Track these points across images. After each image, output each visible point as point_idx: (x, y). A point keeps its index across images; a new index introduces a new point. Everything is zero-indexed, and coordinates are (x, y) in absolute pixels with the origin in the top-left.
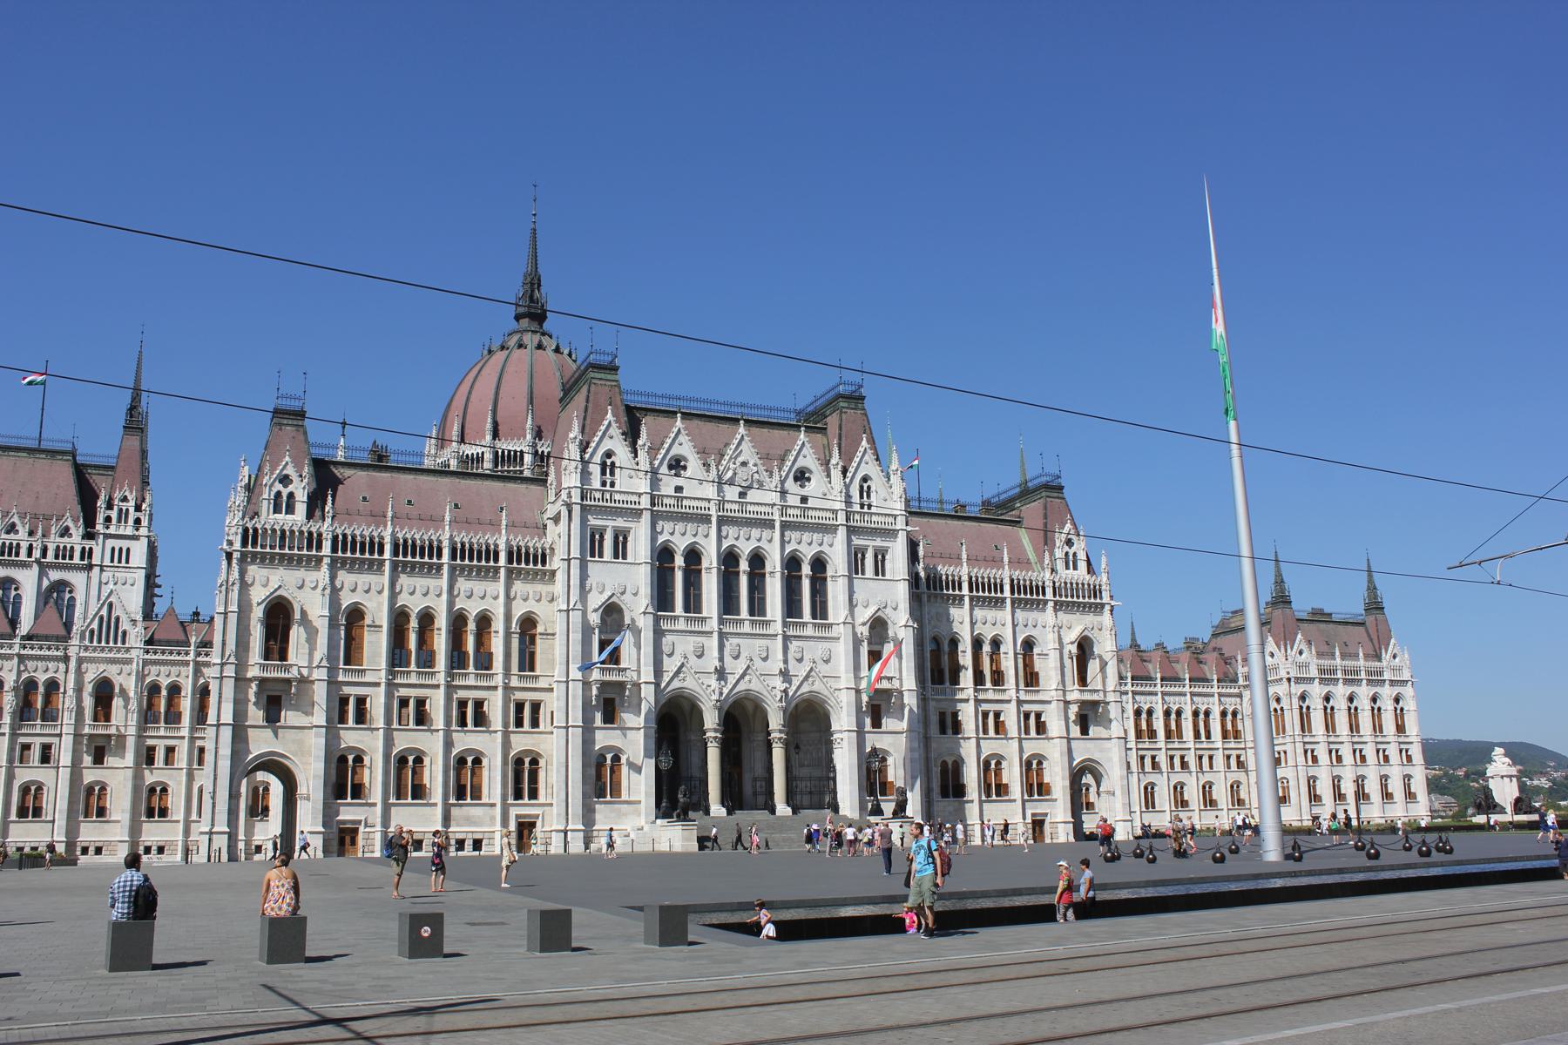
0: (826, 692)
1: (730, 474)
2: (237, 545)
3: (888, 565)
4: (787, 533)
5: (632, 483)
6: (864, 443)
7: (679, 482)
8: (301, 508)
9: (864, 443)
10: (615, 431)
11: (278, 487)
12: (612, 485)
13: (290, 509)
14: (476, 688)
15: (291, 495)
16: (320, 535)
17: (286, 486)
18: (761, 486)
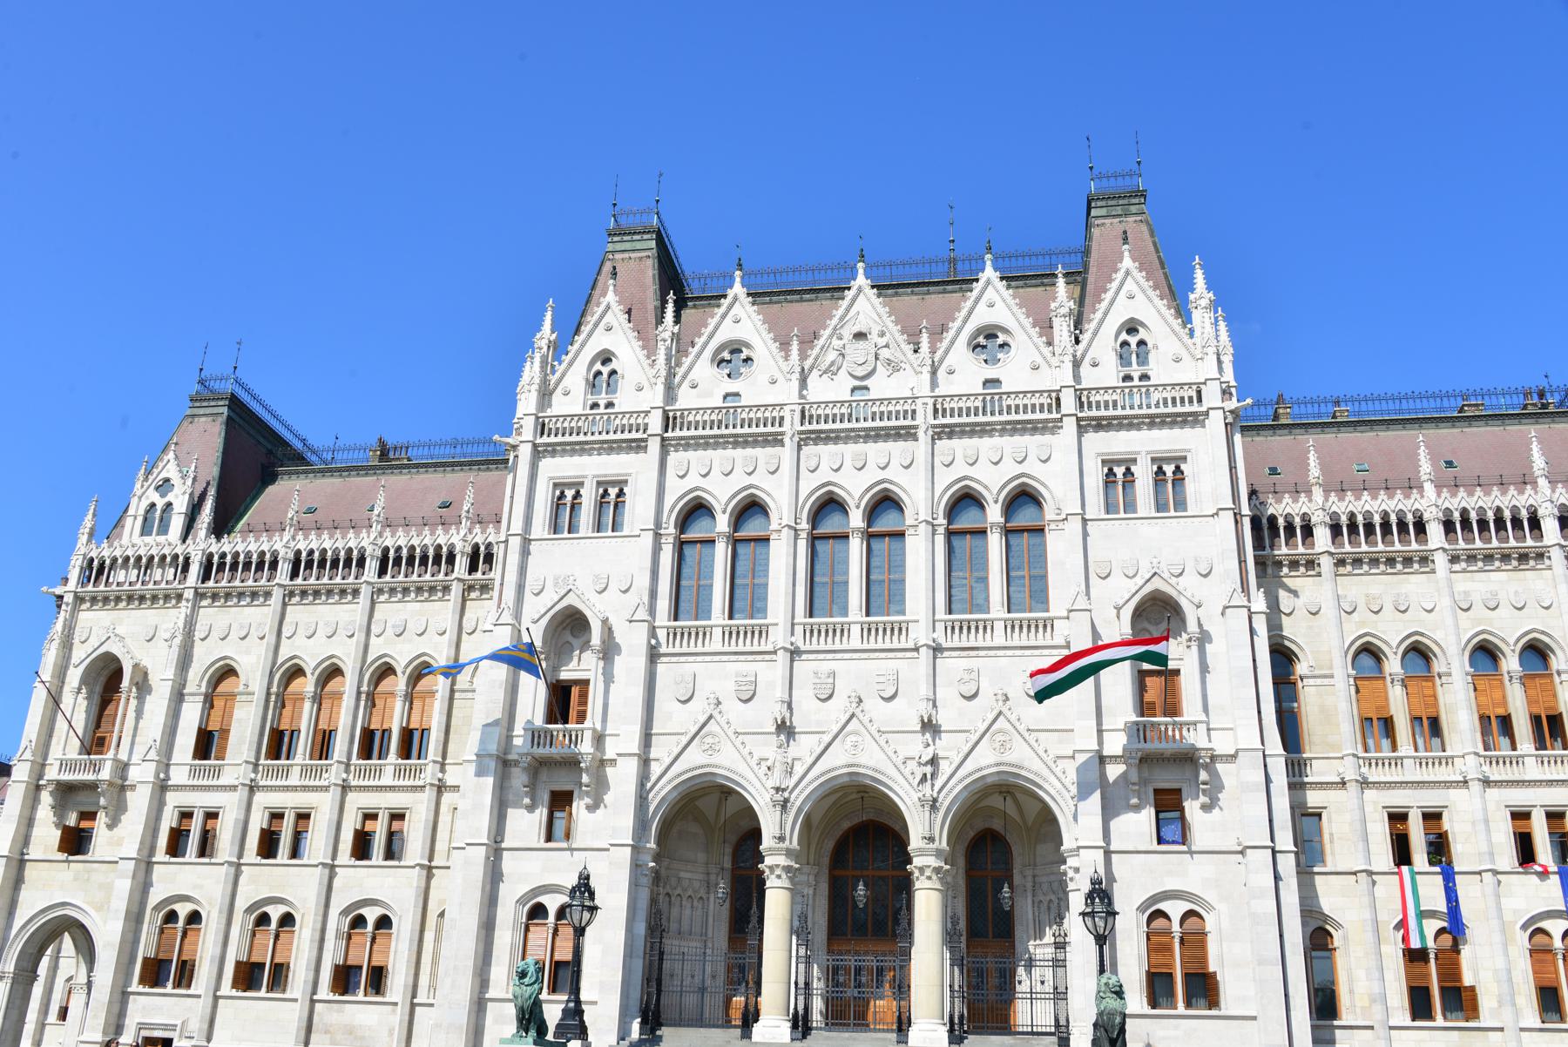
0: (1036, 765)
1: (832, 356)
2: (72, 584)
3: (1190, 487)
4: (943, 445)
5: (638, 393)
6: (1127, 262)
8: (177, 523)
9: (1127, 262)
10: (616, 317)
11: (154, 497)
12: (610, 405)
13: (164, 529)
14: (392, 788)
15: (169, 505)
16: (187, 559)
17: (163, 496)
18: (894, 367)
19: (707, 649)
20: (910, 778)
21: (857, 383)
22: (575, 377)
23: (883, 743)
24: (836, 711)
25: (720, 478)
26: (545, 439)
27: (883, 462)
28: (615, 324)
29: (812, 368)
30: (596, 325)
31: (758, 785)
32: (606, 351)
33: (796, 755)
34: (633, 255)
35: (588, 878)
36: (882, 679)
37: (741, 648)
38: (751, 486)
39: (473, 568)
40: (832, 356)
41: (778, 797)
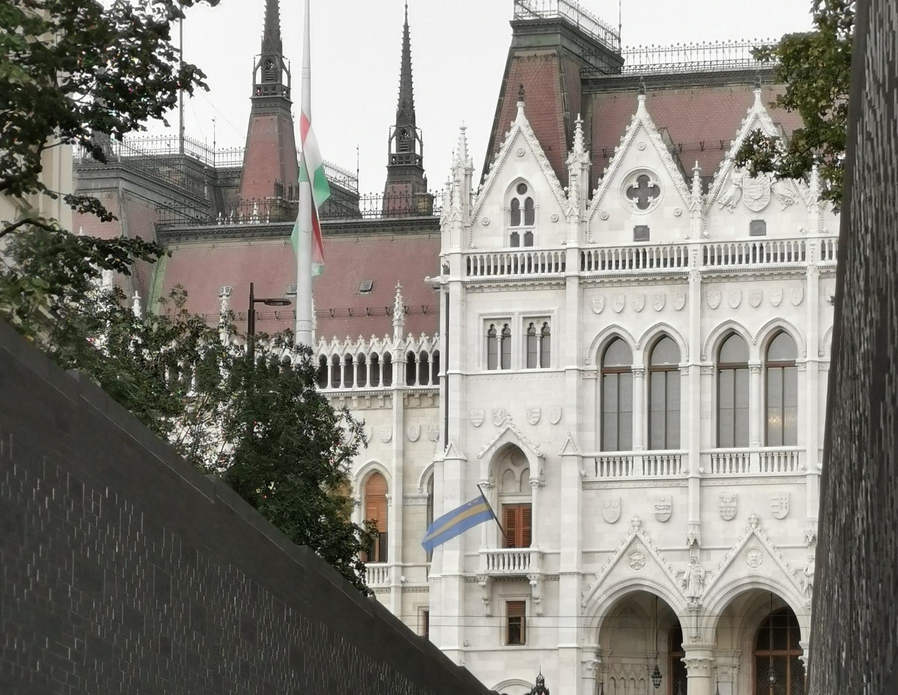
7: (642, 218)
19: (630, 477)
20: (799, 586)
21: (755, 217)
22: (495, 209)
23: (777, 558)
24: (739, 530)
25: (636, 316)
26: (473, 277)
27: (777, 300)
28: (528, 150)
29: (714, 200)
30: (509, 151)
31: (678, 595)
32: (520, 179)
33: (708, 569)
34: (539, 53)
35: (543, 681)
36: (776, 503)
37: (659, 476)
38: (661, 324)
39: (410, 379)
40: (731, 191)
41: (694, 604)
